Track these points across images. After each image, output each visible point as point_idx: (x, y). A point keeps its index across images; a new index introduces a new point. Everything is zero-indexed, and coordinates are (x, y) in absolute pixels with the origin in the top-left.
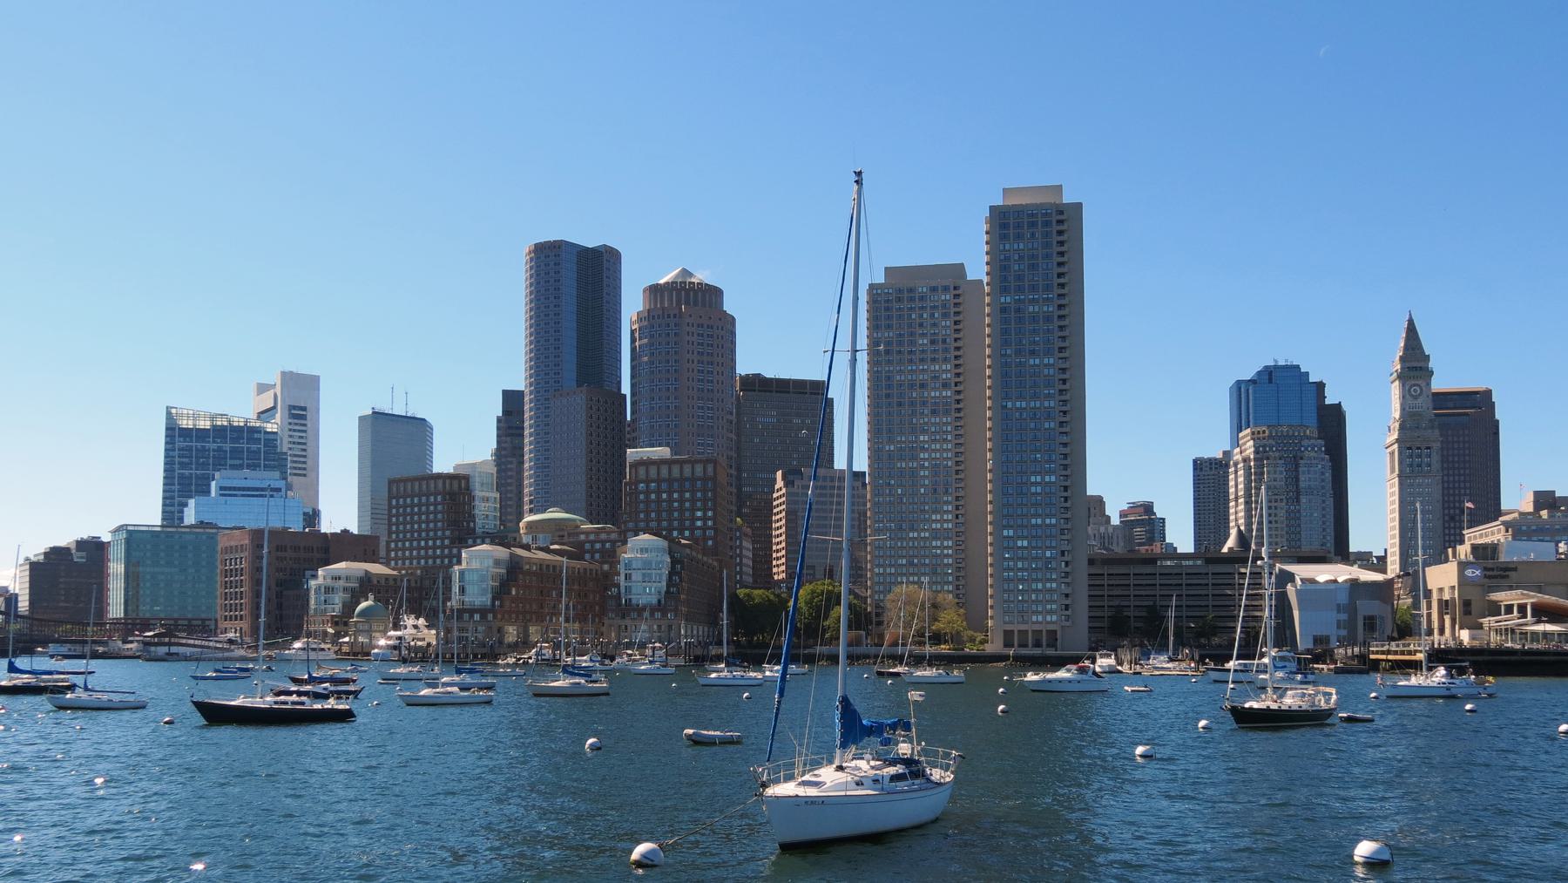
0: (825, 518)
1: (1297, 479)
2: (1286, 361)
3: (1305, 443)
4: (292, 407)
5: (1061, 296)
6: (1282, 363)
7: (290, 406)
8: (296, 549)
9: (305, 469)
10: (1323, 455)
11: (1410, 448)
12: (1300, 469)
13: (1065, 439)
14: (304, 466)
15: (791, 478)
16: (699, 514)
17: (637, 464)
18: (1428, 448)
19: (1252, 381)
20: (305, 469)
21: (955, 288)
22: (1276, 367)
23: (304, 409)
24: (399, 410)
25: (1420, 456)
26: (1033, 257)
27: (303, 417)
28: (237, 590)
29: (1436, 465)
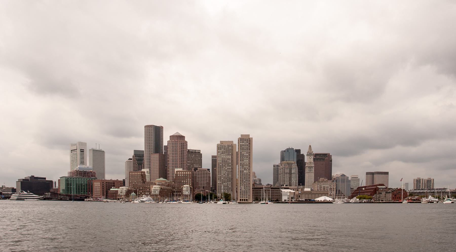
0: (196, 177)
1: (291, 171)
2: (291, 147)
3: (293, 164)
4: (81, 150)
5: (249, 159)
6: (290, 148)
7: (80, 149)
8: (109, 183)
9: (84, 163)
10: (296, 167)
11: (309, 168)
12: (292, 169)
13: (249, 172)
14: (83, 162)
15: (195, 170)
16: (189, 180)
17: (177, 172)
18: (312, 168)
19: (285, 151)
20: (84, 163)
21: (232, 145)
22: (289, 149)
23: (83, 150)
24: (98, 149)
25: (310, 169)
26: (247, 156)
27: (83, 152)
28: (83, 190)
29: (313, 171)
